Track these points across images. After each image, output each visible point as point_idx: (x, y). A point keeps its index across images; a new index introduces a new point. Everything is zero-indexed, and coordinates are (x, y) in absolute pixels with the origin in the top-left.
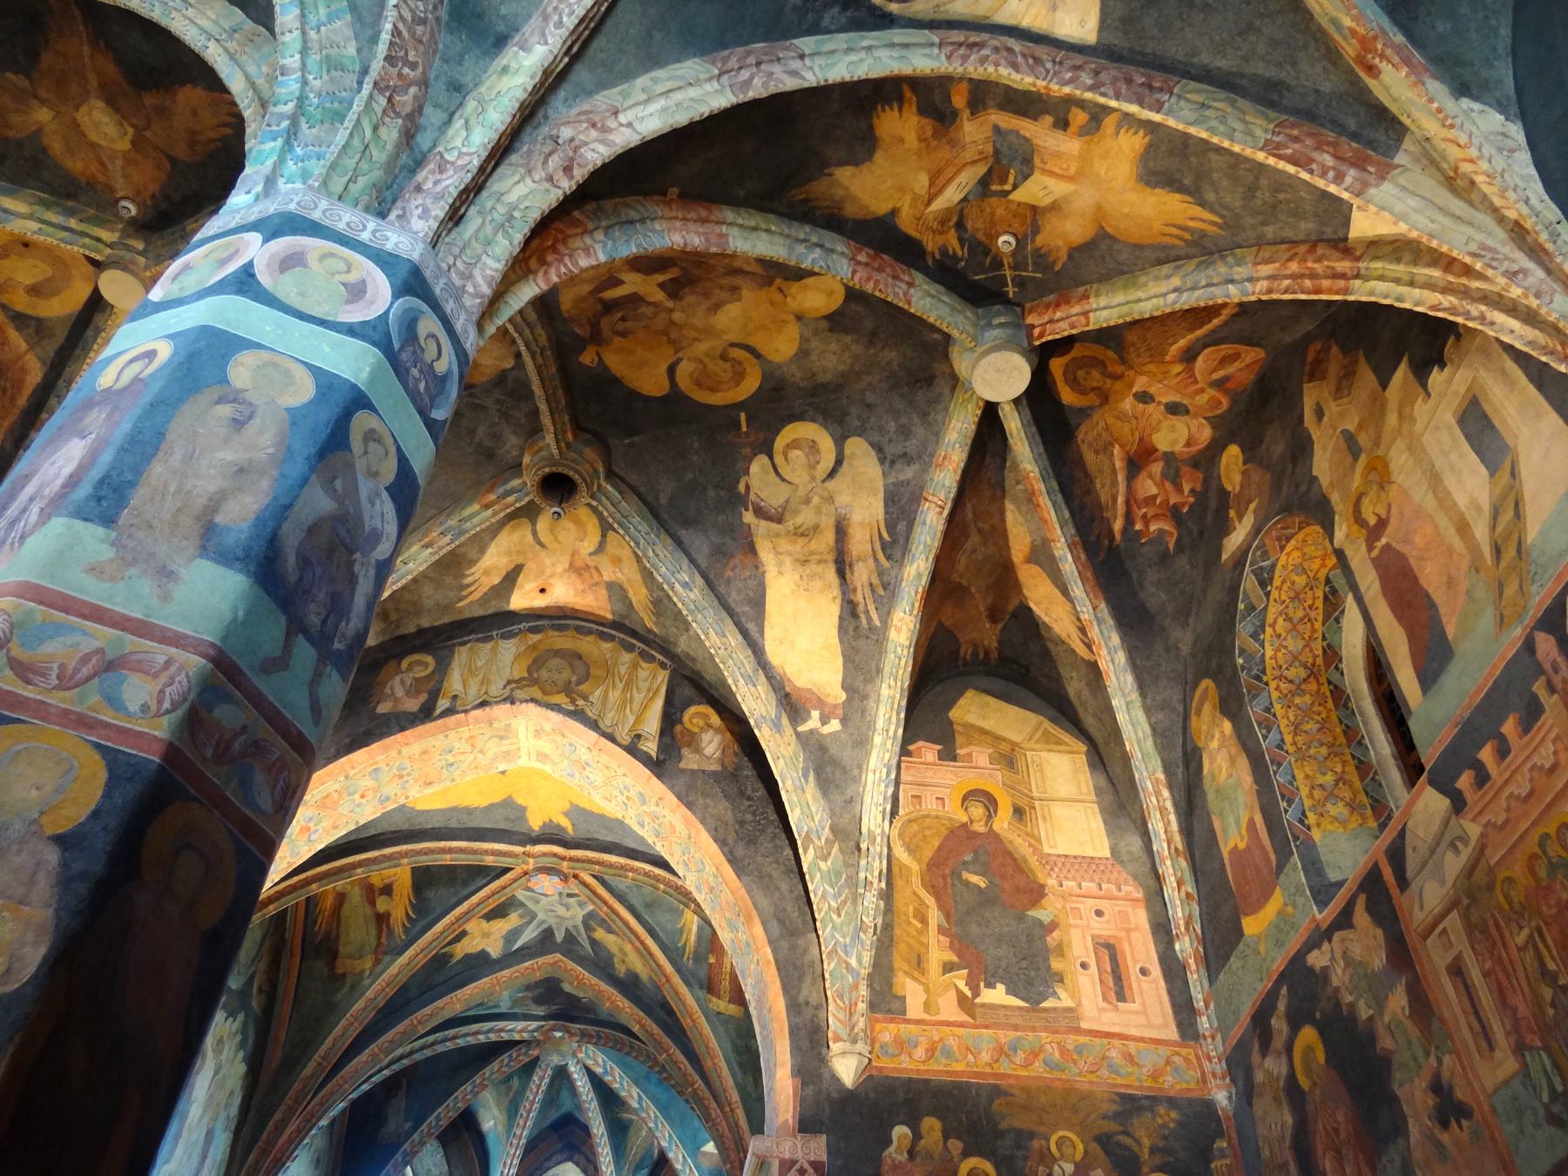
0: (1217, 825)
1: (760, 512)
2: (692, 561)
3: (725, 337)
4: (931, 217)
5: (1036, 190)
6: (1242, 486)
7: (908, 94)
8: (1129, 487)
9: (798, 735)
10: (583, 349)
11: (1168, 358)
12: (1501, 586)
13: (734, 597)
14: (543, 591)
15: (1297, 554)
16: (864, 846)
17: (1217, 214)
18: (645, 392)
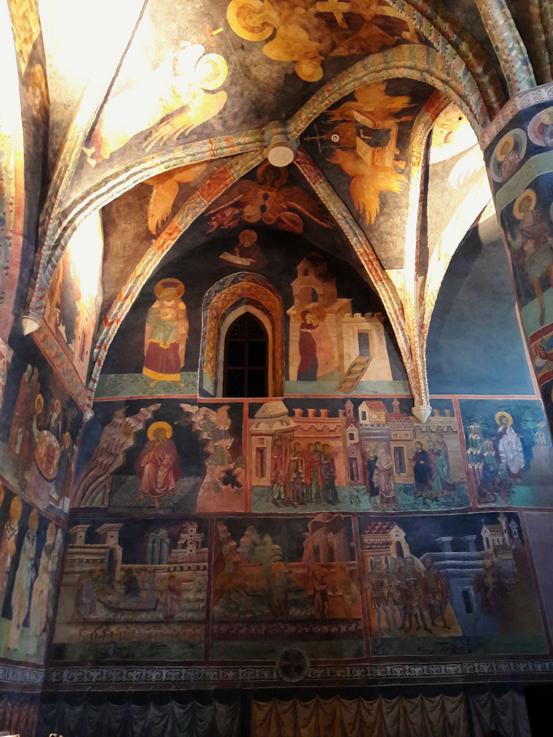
0: (148, 328)
4: (350, 112)
5: (363, 148)
6: (249, 248)
8: (228, 207)
11: (289, 202)
12: (345, 381)
15: (249, 286)
16: (64, 224)
17: (375, 222)
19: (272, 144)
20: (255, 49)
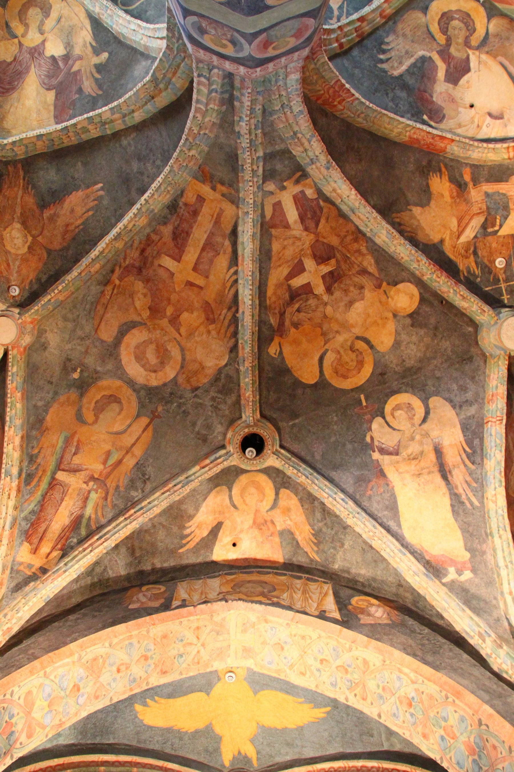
1: (383, 451)
2: (343, 491)
3: (353, 330)
7: (443, 169)
9: (444, 584)
10: (272, 340)
13: (375, 507)
14: (234, 545)
18: (303, 381)
20: (383, 360)
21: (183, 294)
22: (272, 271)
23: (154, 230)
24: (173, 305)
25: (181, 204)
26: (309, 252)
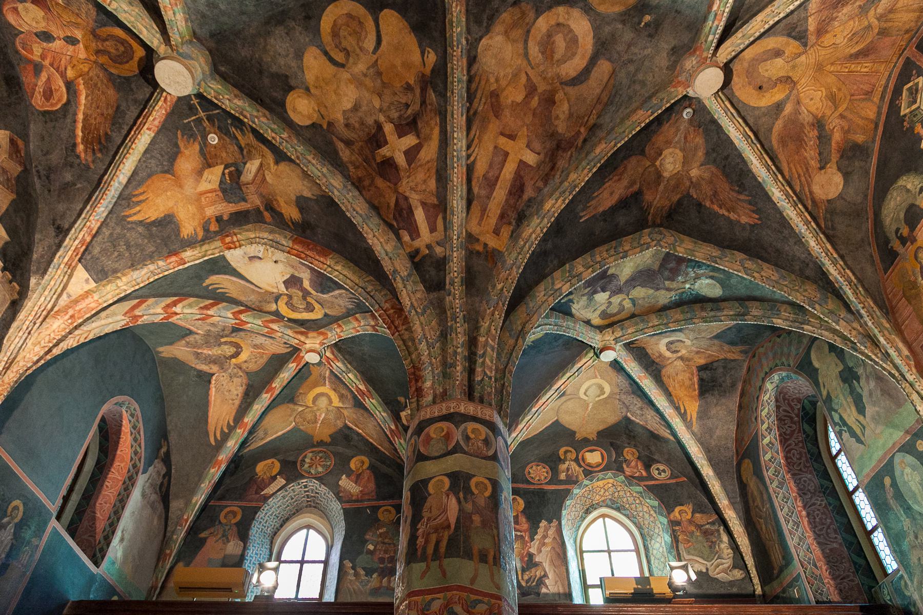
7: (290, 224)
10: (433, 71)
19: (186, 61)
21: (520, 123)
22: (435, 156)
23: (540, 191)
24: (530, 109)
25: (514, 223)
26: (402, 174)
